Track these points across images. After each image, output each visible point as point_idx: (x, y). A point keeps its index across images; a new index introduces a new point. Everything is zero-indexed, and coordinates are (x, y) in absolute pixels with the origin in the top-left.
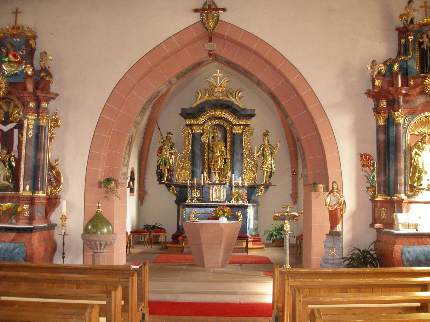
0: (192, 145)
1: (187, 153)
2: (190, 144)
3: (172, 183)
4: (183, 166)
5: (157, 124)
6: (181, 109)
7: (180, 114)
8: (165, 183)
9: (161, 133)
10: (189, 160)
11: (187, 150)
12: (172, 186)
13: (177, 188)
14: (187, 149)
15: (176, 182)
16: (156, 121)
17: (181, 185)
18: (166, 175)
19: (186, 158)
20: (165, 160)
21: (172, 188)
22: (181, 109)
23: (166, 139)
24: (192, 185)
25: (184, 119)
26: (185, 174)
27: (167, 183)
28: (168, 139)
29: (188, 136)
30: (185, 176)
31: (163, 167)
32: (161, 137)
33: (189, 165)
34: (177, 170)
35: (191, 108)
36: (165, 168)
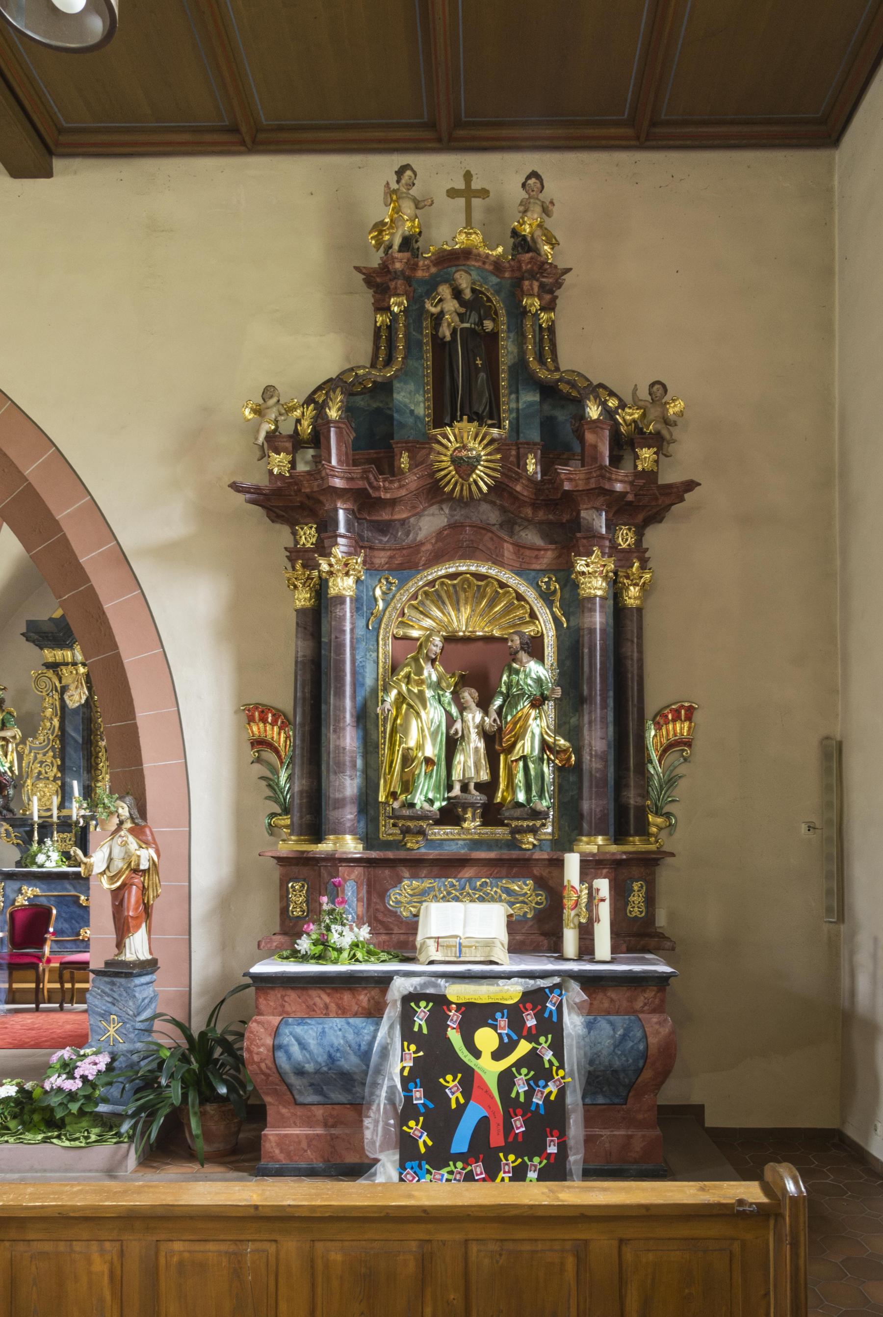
0: (61, 717)
1: (49, 739)
2: (56, 716)
4: (40, 773)
6: (27, 621)
7: (23, 634)
10: (54, 757)
11: (49, 730)
19: (47, 752)
22: (27, 621)
33: (55, 769)
34: (25, 782)
35: (51, 619)
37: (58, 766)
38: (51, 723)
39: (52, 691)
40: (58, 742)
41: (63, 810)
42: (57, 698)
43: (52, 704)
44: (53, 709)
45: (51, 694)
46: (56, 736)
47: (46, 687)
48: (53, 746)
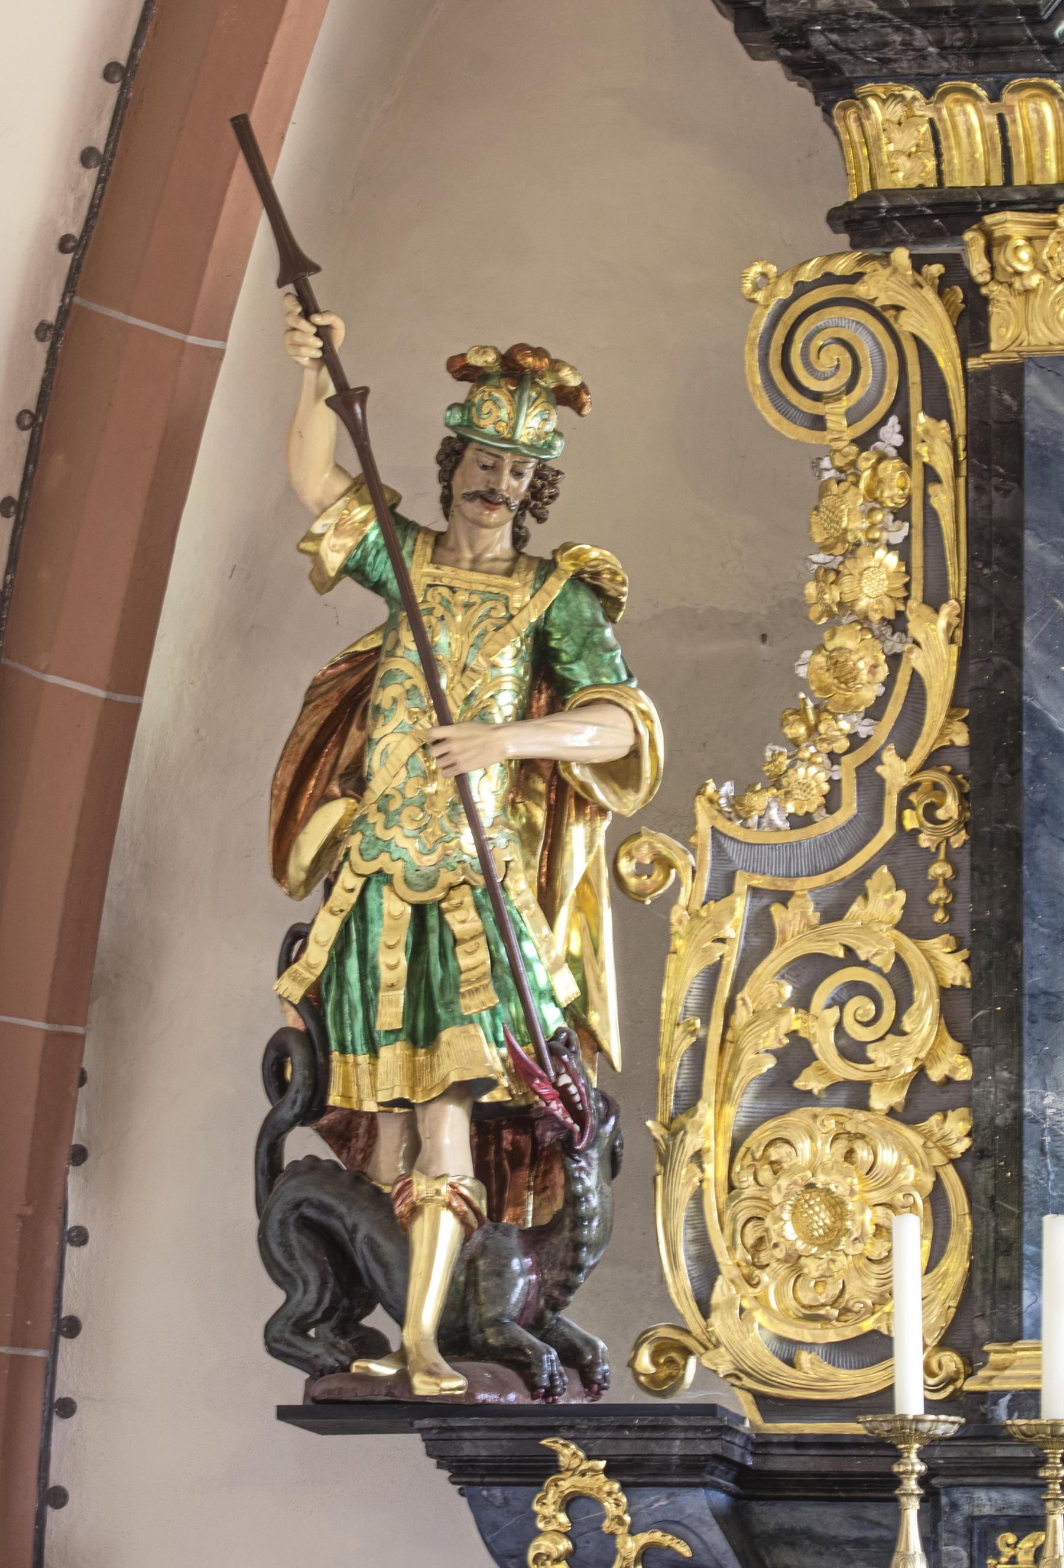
0: (970, 614)
2: (934, 601)
3: (571, 1395)
5: (241, 169)
8: (423, 1386)
9: (329, 359)
11: (875, 712)
12: (568, 1453)
13: (658, 1500)
14: (870, 693)
15: (654, 1385)
16: (241, 127)
17: (761, 1444)
18: (449, 1228)
20: (419, 911)
21: (570, 1503)
23: (447, 501)
24: (997, 1434)
25: (801, 96)
26: (836, 1205)
27: (453, 1384)
28: (489, 498)
29: (891, 435)
30: (831, 1239)
31: (392, 1055)
32: (355, 468)
34: (674, 1129)
36: (414, 1078)
37: (947, 994)
38: (894, 660)
39: (900, 407)
40: (950, 808)
41: (996, 1353)
42: (943, 465)
43: (901, 514)
44: (903, 550)
45: (891, 435)
46: (932, 761)
47: (850, 386)
48: (906, 837)
